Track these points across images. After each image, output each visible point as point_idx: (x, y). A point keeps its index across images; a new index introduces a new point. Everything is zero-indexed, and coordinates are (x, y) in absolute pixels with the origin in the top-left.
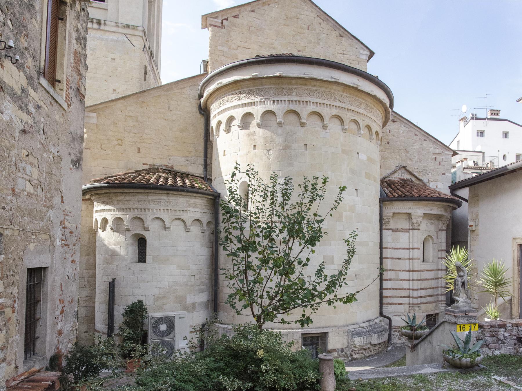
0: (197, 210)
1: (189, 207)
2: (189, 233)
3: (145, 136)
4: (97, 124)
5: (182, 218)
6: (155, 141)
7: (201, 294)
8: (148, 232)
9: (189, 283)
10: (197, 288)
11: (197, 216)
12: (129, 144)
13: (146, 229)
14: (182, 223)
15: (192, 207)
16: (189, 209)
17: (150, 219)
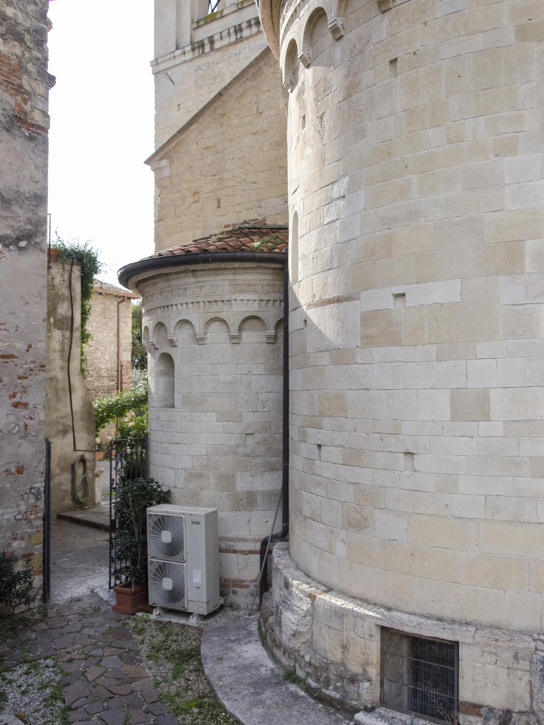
0: (252, 297)
1: (234, 293)
2: (237, 347)
3: (226, 176)
4: (170, 177)
5: (221, 316)
6: (239, 180)
7: (266, 474)
8: (175, 349)
9: (241, 450)
10: (258, 460)
11: (253, 308)
12: (207, 198)
13: (172, 343)
14: (224, 328)
15: (242, 292)
16: (234, 297)
17: (173, 323)
